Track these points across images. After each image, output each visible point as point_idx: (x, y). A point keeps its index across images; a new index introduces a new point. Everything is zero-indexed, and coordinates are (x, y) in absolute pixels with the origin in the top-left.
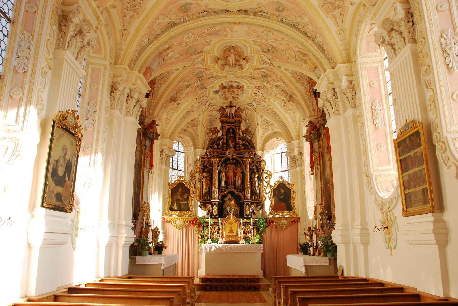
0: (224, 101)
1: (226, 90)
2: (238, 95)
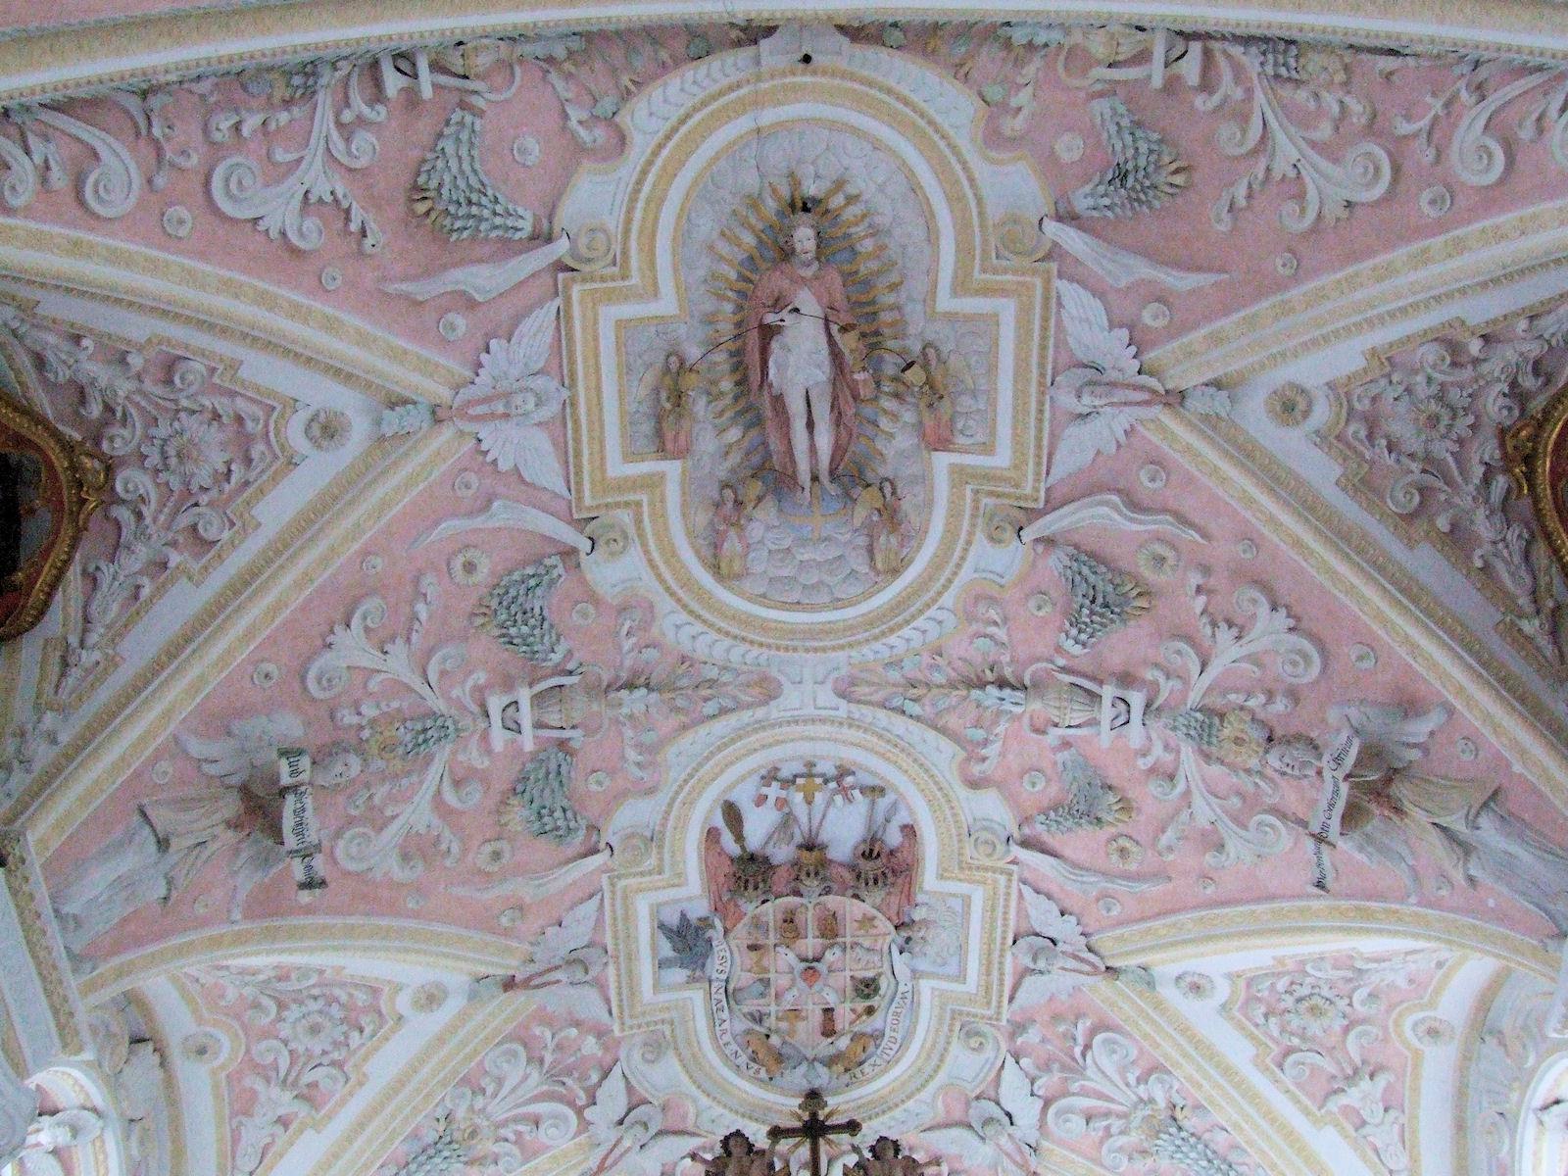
0: (750, 1090)
1: (772, 911)
2: (867, 988)
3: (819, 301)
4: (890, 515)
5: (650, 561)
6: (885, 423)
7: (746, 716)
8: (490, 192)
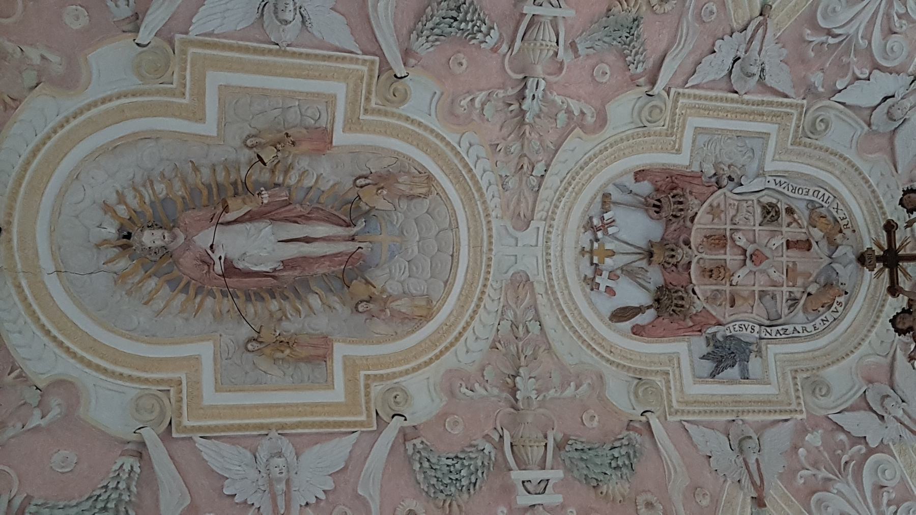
1: (703, 288)
2: (770, 213)
3: (203, 228)
4: (383, 181)
5: (415, 370)
6: (309, 182)
7: (542, 301)
8: (97, 492)
